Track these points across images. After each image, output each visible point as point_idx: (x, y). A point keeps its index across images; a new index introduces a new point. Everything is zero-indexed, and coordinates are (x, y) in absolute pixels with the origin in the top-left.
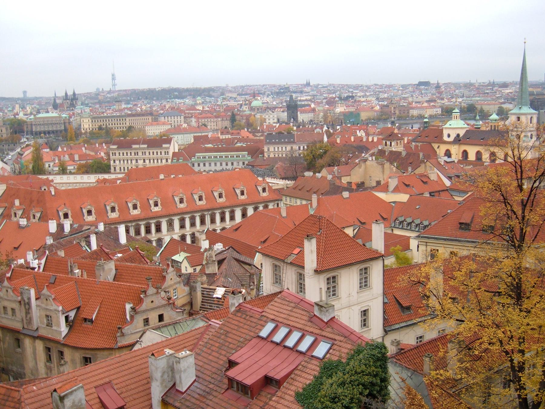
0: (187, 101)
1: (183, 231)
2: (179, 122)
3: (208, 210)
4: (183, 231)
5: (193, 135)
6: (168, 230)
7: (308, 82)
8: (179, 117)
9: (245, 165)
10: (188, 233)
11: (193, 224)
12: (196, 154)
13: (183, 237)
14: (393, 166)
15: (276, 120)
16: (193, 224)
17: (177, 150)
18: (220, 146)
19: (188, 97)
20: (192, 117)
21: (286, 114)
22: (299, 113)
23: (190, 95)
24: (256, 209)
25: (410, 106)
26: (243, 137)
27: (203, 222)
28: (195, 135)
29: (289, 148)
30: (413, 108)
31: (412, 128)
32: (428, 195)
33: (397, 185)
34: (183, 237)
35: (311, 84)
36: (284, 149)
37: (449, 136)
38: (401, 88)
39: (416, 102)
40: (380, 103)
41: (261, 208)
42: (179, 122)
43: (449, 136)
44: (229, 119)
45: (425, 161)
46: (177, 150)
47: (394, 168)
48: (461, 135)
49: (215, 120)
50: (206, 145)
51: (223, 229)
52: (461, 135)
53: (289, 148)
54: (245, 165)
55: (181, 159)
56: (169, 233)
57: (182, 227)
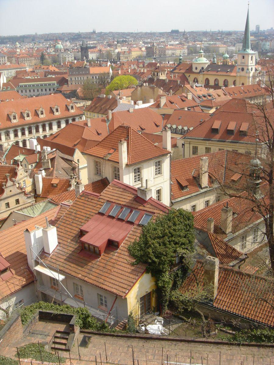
0: (8, 45)
1: (17, 139)
2: (4, 61)
3: (34, 123)
4: (17, 139)
5: (15, 70)
6: (6, 139)
7: (94, 30)
8: (3, 57)
9: (55, 90)
10: (20, 141)
11: (23, 134)
12: (20, 84)
13: (17, 143)
14: (160, 90)
15: (73, 58)
16: (23, 134)
17: (5, 82)
18: (36, 78)
19: (8, 43)
20: (13, 57)
21: (80, 53)
22: (89, 53)
23: (10, 41)
24: (67, 122)
25: (166, 47)
26: (51, 71)
27: (30, 132)
28: (16, 70)
29: (85, 78)
30: (168, 49)
31: (169, 63)
32: (187, 110)
33: (165, 103)
34: (17, 143)
35: (96, 32)
36: (82, 79)
37: (196, 69)
38: (159, 35)
39: (170, 45)
40: (146, 45)
41: (70, 121)
42: (4, 61)
43: (196, 69)
44: (39, 58)
45: (183, 86)
46: (5, 82)
47: (162, 91)
48: (205, 68)
49: (30, 59)
50: (26, 77)
51: (45, 136)
52: (205, 68)
53: (85, 78)
54: (55, 90)
55: (9, 88)
56: (7, 141)
57: (16, 135)
